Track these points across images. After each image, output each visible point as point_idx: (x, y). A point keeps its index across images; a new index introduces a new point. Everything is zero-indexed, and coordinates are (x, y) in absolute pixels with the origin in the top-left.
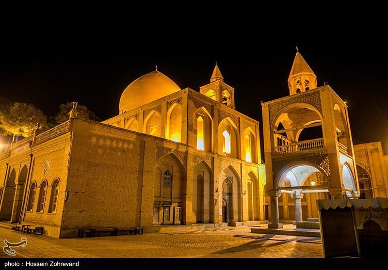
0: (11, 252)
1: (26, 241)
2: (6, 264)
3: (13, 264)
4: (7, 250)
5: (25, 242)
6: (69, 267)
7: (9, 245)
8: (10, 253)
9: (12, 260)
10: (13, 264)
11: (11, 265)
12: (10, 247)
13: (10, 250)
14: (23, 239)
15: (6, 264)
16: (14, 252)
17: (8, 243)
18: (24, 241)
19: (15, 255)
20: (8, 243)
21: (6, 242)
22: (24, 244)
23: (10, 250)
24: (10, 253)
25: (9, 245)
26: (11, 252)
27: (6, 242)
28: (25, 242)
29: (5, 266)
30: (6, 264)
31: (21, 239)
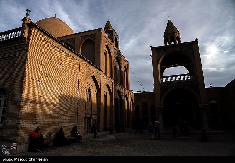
0: (7, 152)
1: (16, 145)
2: (4, 160)
3: (8, 160)
4: (4, 151)
5: (15, 146)
6: (39, 161)
7: (5, 148)
8: (7, 153)
9: (7, 157)
10: (8, 160)
11: (7, 160)
12: (5, 149)
13: (6, 151)
14: (14, 144)
15: (4, 160)
16: (8, 152)
17: (4, 147)
18: (15, 145)
19: (9, 154)
20: (4, 147)
21: (3, 146)
22: (15, 147)
23: (6, 151)
24: (7, 153)
25: (5, 148)
26: (7, 152)
27: (3, 146)
28: (15, 146)
29: (3, 160)
30: (4, 160)
31: (13, 145)
